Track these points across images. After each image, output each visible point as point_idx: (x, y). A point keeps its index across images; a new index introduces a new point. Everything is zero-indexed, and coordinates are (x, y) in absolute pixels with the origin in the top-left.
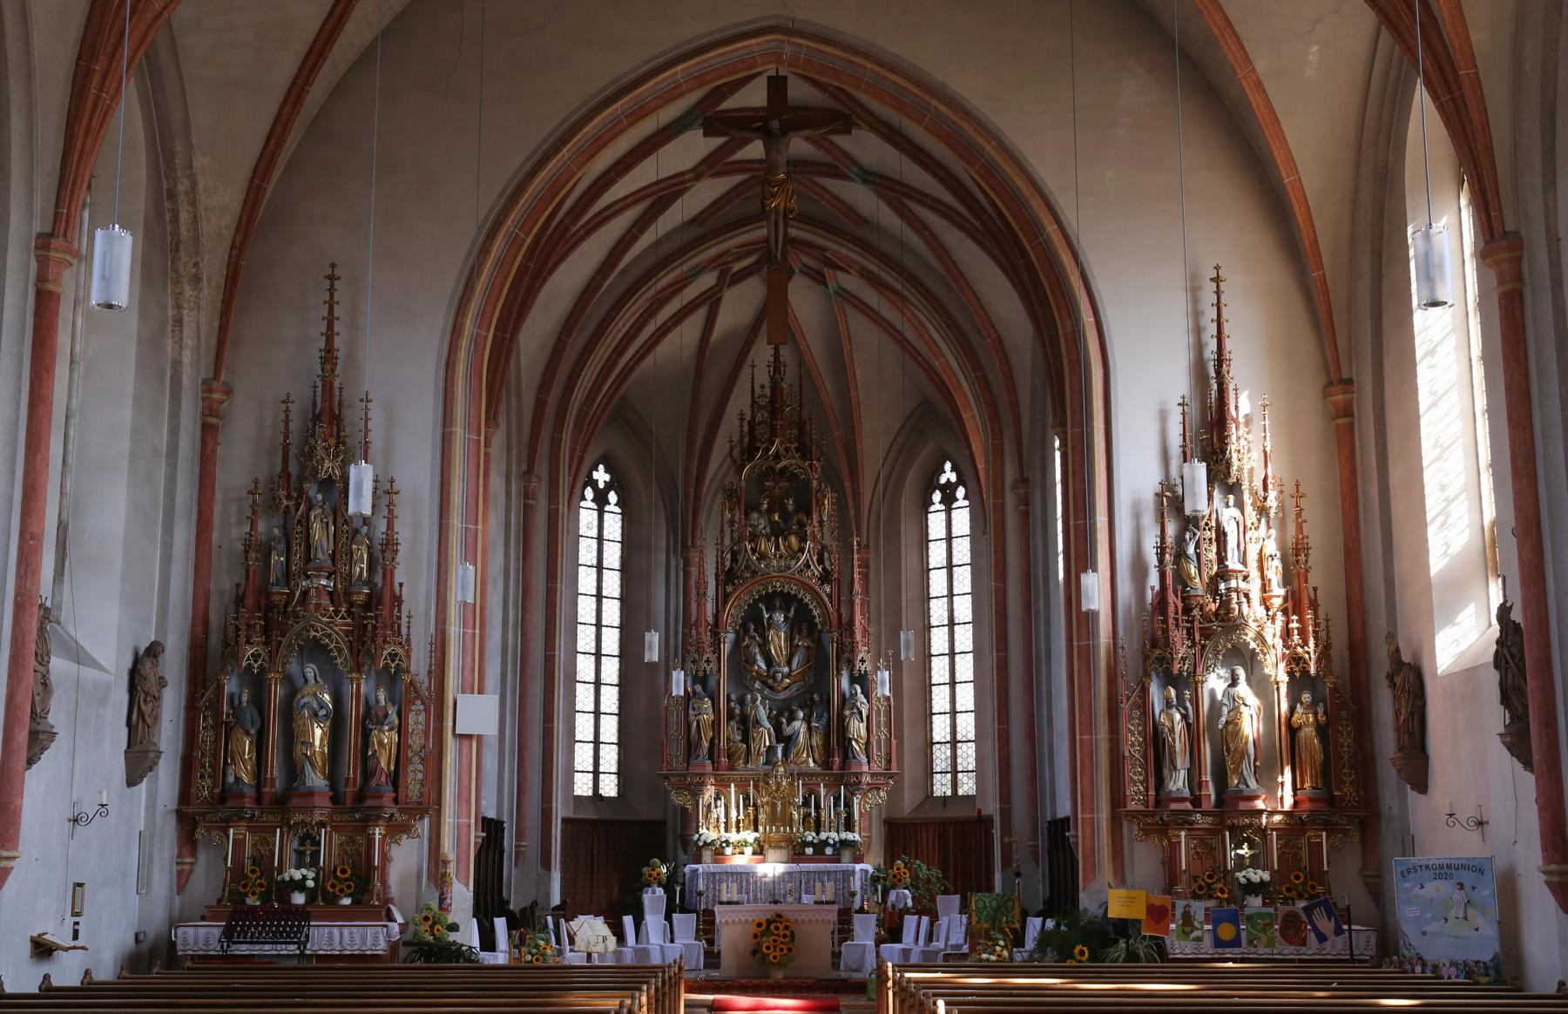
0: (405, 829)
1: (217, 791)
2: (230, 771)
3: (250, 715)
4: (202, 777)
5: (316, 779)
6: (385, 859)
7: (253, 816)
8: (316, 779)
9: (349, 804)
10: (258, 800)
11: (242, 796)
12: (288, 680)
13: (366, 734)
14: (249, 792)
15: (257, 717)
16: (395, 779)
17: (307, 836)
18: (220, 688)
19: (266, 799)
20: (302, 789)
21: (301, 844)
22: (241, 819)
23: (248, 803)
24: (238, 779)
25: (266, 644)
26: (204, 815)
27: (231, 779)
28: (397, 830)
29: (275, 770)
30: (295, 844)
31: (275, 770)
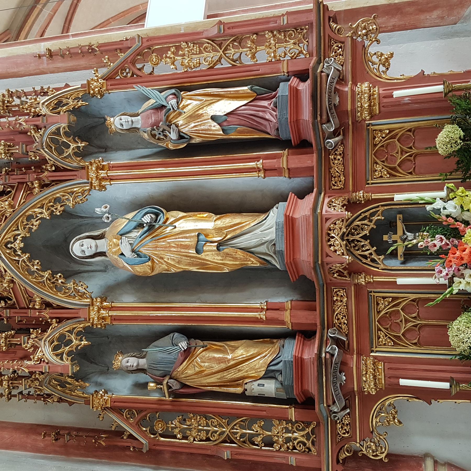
0: (359, 54)
1: (292, 413)
2: (254, 388)
3: (157, 352)
4: (269, 443)
5: (264, 230)
6: (421, 79)
7: (337, 342)
8: (264, 230)
9: (309, 160)
10: (307, 334)
11: (299, 363)
12: (108, 293)
13: (193, 149)
14: (290, 350)
15: (167, 339)
16: (265, 86)
17: (375, 238)
18: (117, 408)
19: (306, 318)
20: (281, 246)
21: (394, 255)
22: (343, 366)
23: (310, 354)
24: (269, 374)
25: (44, 326)
26: (340, 443)
27: (270, 387)
28: (359, 66)
29: (251, 305)
30: (394, 263)
31: (251, 305)
